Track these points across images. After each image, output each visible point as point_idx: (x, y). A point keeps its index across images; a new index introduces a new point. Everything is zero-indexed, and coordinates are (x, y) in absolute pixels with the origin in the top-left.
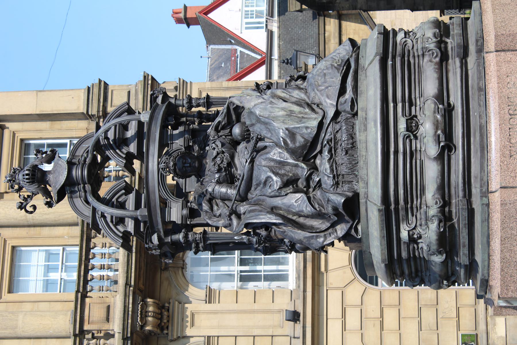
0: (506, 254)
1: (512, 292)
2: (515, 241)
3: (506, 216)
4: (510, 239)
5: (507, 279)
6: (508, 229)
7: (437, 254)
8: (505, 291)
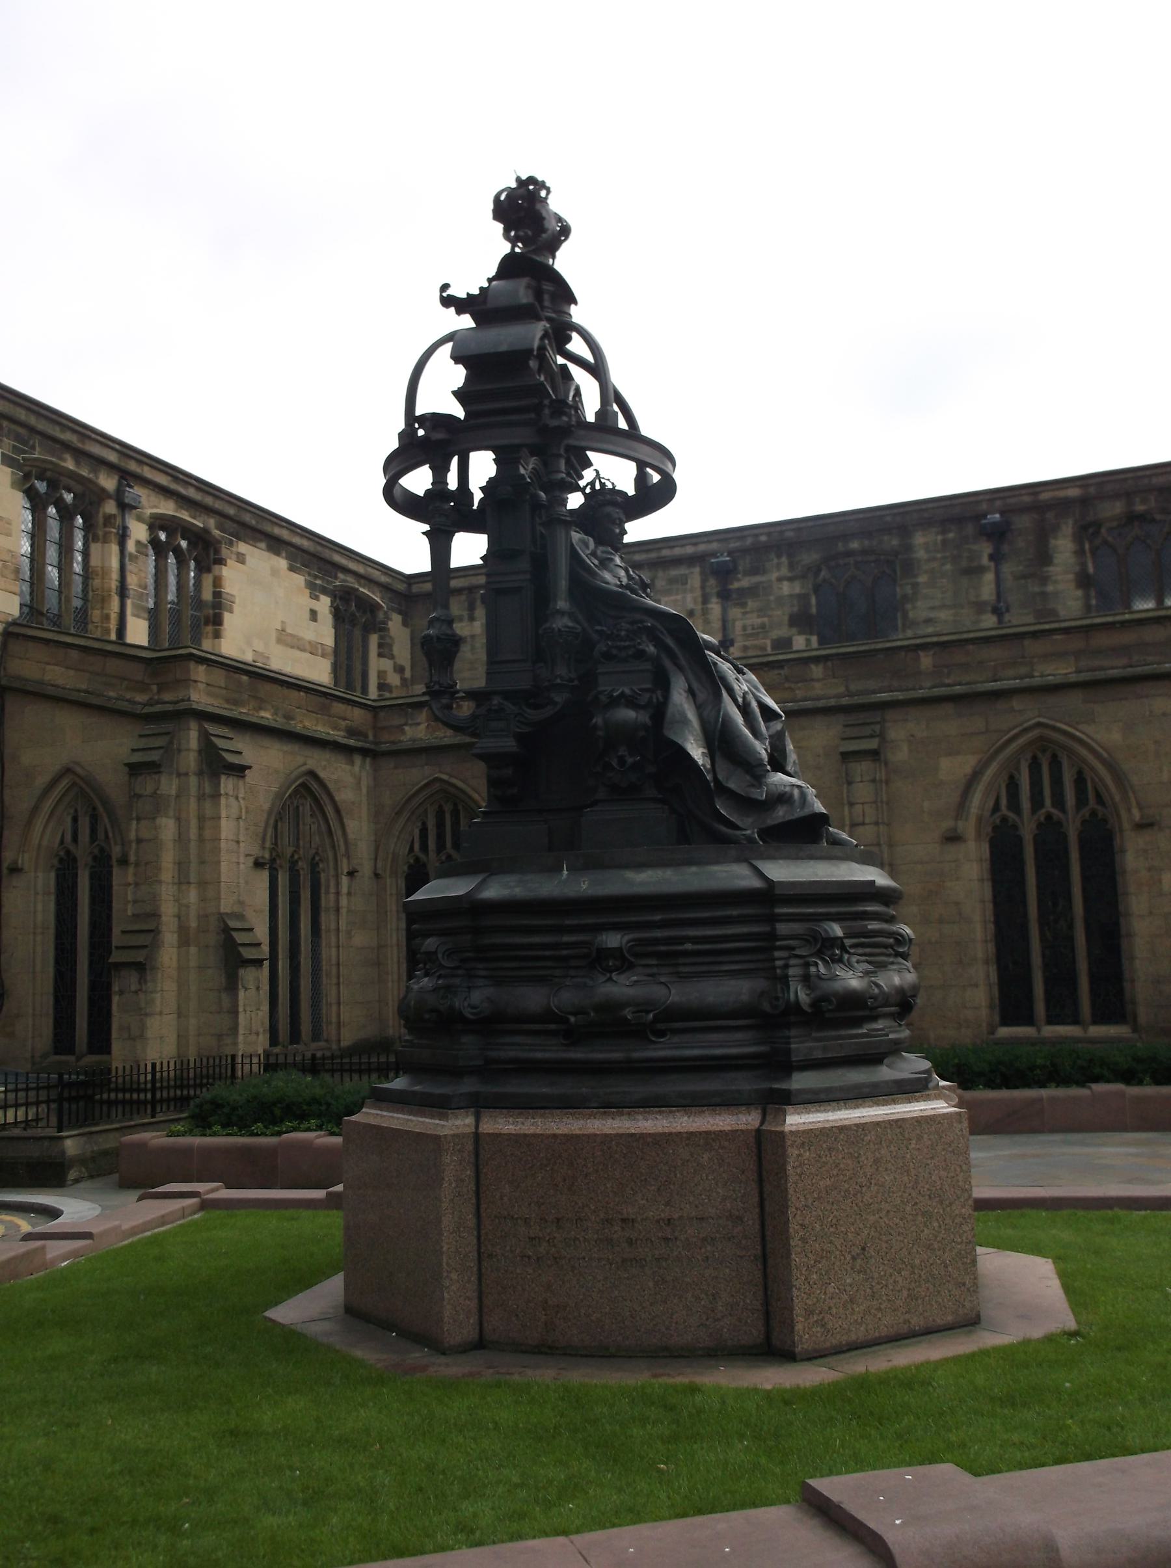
0: (873, 1133)
1: (799, 1155)
2: (896, 1149)
3: (940, 1125)
4: (901, 1137)
5: (825, 1142)
6: (918, 1132)
7: (812, 996)
8: (799, 1141)
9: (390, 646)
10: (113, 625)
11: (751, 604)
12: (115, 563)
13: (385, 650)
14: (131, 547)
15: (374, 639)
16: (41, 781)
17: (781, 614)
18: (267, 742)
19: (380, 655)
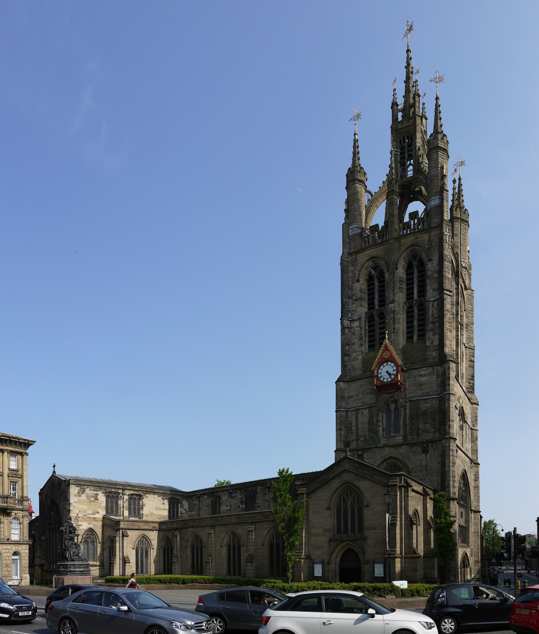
9: (183, 506)
10: (122, 512)
11: (235, 499)
12: (122, 503)
13: (182, 507)
14: (125, 500)
15: (180, 505)
16: (107, 538)
17: (238, 501)
18: (135, 531)
19: (181, 508)
